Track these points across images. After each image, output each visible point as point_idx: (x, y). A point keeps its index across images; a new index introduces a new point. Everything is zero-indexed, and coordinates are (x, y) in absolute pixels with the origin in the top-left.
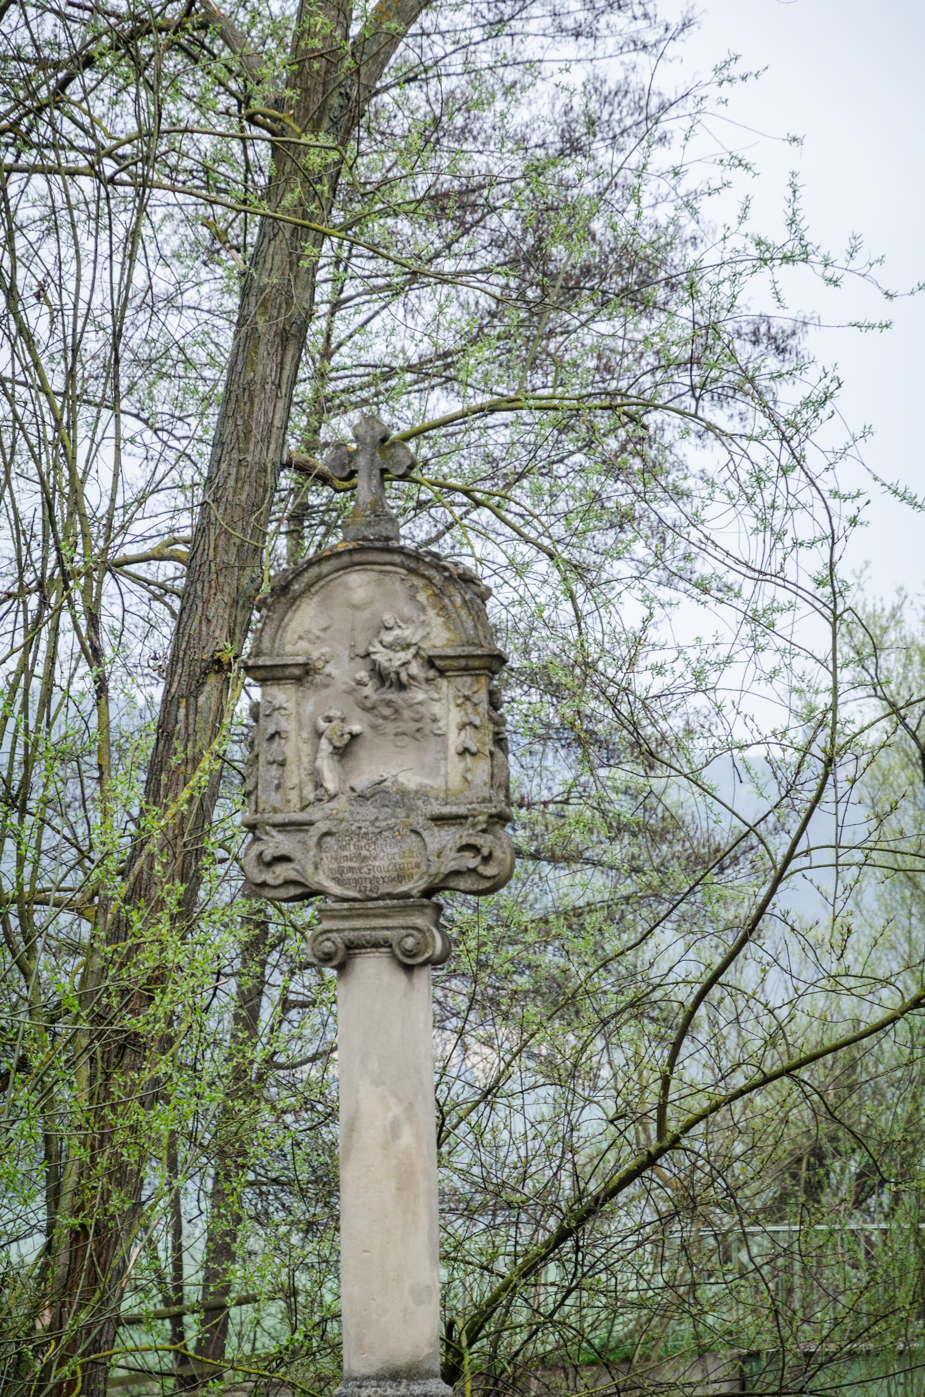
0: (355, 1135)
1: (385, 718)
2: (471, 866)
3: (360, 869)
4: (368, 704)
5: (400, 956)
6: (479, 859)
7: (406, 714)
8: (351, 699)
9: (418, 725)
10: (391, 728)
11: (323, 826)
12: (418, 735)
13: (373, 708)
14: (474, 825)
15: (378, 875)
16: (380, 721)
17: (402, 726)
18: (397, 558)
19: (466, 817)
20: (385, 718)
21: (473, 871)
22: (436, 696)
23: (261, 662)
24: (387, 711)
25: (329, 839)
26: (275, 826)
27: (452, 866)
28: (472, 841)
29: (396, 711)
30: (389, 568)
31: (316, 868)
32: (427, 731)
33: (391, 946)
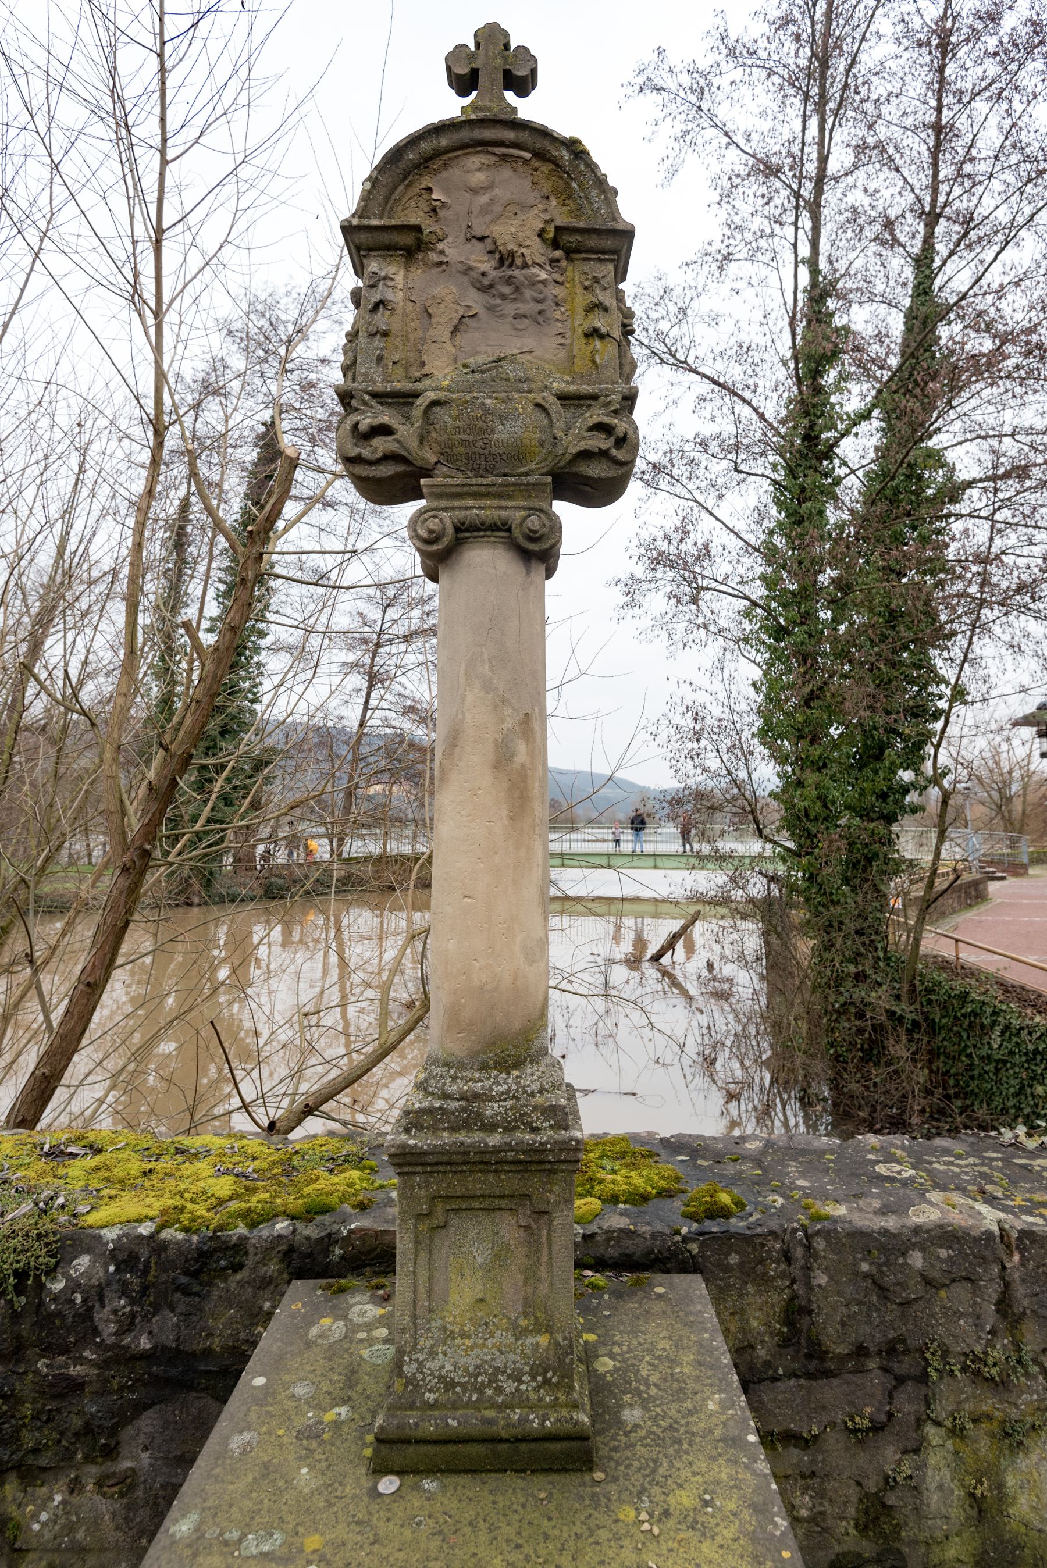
0: (457, 750)
1: (503, 297)
2: (604, 447)
3: (475, 442)
4: (486, 282)
5: (522, 541)
6: (612, 440)
7: (528, 293)
8: (465, 279)
9: (540, 307)
10: (509, 309)
11: (432, 395)
12: (540, 319)
13: (491, 286)
14: (607, 405)
15: (494, 450)
16: (498, 301)
17: (523, 308)
18: (524, 136)
19: (595, 397)
20: (503, 297)
21: (604, 454)
22: (560, 279)
23: (366, 222)
24: (506, 290)
25: (437, 410)
26: (375, 395)
27: (583, 445)
28: (606, 420)
29: (517, 289)
30: (512, 151)
31: (421, 442)
32: (548, 314)
33: (509, 530)
